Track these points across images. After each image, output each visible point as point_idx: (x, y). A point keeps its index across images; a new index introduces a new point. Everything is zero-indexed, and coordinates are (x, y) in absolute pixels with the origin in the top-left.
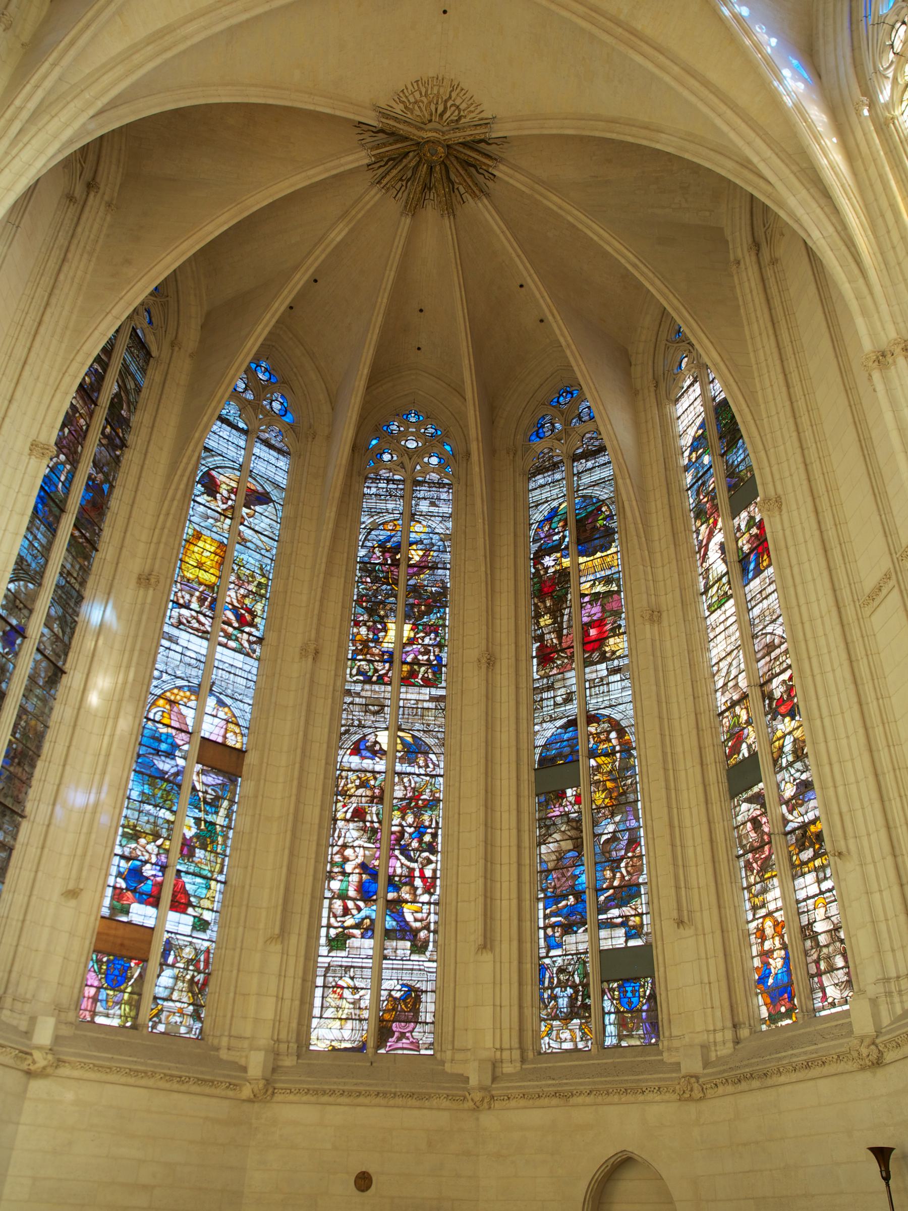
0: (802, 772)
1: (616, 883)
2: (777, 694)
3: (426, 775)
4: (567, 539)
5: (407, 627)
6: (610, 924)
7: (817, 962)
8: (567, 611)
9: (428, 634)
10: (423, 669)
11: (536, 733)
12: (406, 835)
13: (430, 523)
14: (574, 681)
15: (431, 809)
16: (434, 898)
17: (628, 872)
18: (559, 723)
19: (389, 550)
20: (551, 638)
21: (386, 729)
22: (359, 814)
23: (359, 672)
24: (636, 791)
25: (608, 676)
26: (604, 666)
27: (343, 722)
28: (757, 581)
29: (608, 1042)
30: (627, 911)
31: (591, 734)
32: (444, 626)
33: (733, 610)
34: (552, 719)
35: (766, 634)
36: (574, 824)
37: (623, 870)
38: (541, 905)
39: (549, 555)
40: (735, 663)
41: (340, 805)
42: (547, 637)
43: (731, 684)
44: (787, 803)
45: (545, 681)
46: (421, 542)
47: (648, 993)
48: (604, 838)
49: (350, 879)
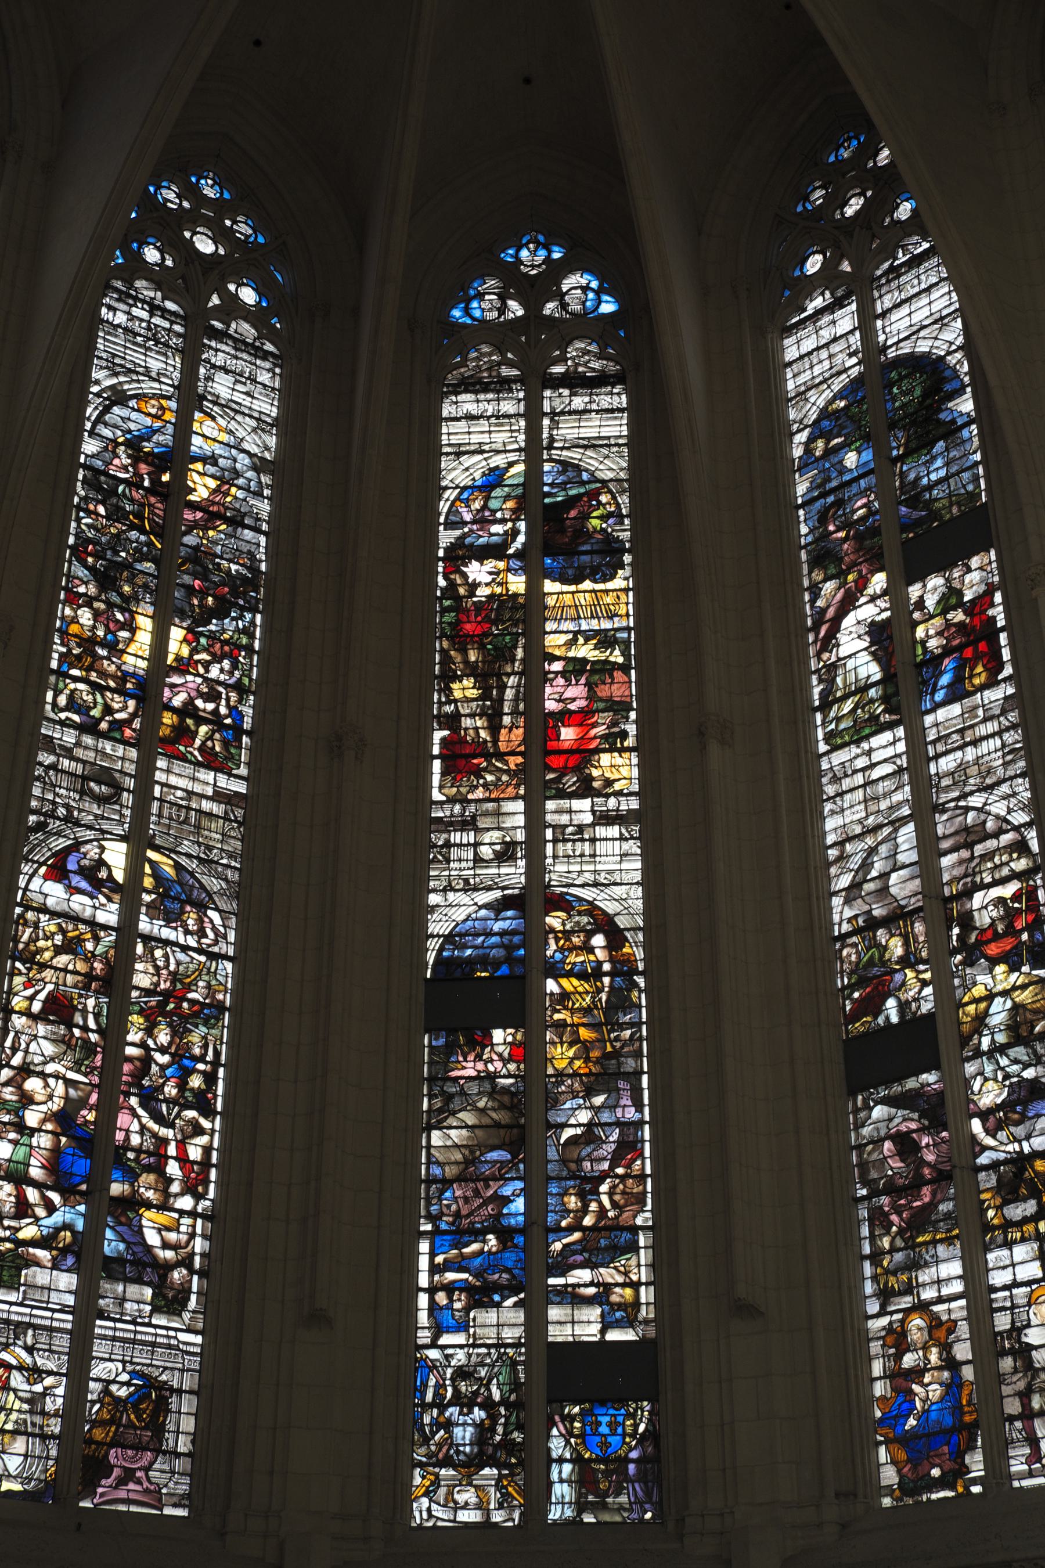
0: (1026, 1066)
1: (588, 1221)
2: (983, 919)
3: (200, 951)
4: (521, 539)
5: (177, 634)
6: (572, 1297)
7: (1025, 1396)
8: (512, 681)
9: (217, 659)
10: (203, 729)
11: (433, 908)
12: (154, 1069)
13: (233, 425)
14: (520, 820)
16: (204, 1205)
17: (614, 1204)
18: (484, 897)
19: (150, 458)
20: (474, 726)
21: (123, 838)
22: (59, 1009)
23: (73, 704)
24: (638, 1055)
25: (593, 825)
26: (585, 804)
27: (34, 803)
28: (956, 709)
29: (555, 1514)
30: (608, 1275)
31: (552, 930)
32: (250, 650)
33: (904, 749)
34: (469, 888)
35: (967, 809)
36: (506, 1099)
37: (605, 1200)
38: (424, 1246)
39: (481, 560)
40: (883, 850)
41: (18, 980)
42: (467, 722)
43: (869, 887)
44: (984, 1115)
45: (457, 808)
46: (211, 460)
47: (642, 1428)
48: (567, 1133)
49: (34, 1141)
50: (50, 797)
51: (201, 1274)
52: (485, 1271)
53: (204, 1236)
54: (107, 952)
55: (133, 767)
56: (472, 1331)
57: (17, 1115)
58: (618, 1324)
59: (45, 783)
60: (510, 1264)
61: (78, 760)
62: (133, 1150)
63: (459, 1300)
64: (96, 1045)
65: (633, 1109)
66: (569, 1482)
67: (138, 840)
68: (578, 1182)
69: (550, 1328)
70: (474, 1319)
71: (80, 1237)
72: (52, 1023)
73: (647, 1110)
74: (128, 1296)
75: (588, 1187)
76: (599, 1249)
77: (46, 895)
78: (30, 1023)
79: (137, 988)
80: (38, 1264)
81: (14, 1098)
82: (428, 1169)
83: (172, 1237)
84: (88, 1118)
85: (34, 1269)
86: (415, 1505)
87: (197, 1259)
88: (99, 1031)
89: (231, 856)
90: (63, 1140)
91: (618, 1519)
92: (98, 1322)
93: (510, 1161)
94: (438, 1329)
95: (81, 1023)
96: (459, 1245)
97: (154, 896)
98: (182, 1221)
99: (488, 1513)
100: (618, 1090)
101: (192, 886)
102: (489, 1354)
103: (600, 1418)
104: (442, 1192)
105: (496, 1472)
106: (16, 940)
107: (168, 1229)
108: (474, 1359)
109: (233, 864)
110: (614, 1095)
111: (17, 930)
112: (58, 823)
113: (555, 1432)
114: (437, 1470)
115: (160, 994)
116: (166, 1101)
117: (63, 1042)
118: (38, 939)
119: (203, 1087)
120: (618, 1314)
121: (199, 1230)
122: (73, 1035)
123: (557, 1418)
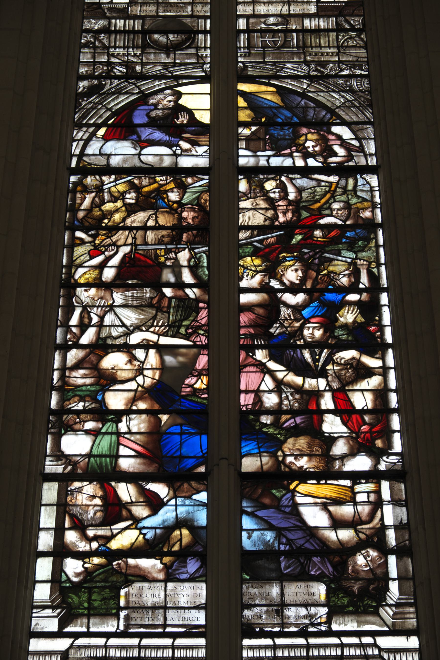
3: (326, 170)
12: (284, 312)
15: (351, 246)
21: (202, 80)
22: (139, 272)
27: (83, 70)
49: (123, 427)
50: (104, 59)
51: (400, 552)
53: (395, 502)
54: (198, 198)
55: (208, 8)
57: (94, 399)
59: (95, 47)
61: (134, 17)
62: (268, 412)
64: (197, 300)
67: (223, 80)
71: (203, 533)
72: (133, 287)
74: (288, 598)
77: (109, 156)
78: (102, 293)
79: (246, 228)
80: (144, 577)
81: (88, 381)
83: (347, 511)
84: (198, 386)
85: (138, 585)
87: (391, 535)
88: (200, 284)
89: (352, 65)
90: (164, 418)
92: (246, 642)
95: (172, 279)
97: (254, 128)
98: (358, 488)
101: (307, 107)
106: (74, 209)
107: (338, 502)
109: (358, 72)
111: (74, 199)
112: (116, 82)
115: (281, 227)
116: (310, 345)
117: (150, 305)
118: (103, 202)
119: (360, 319)
121: (386, 495)
122: (164, 295)
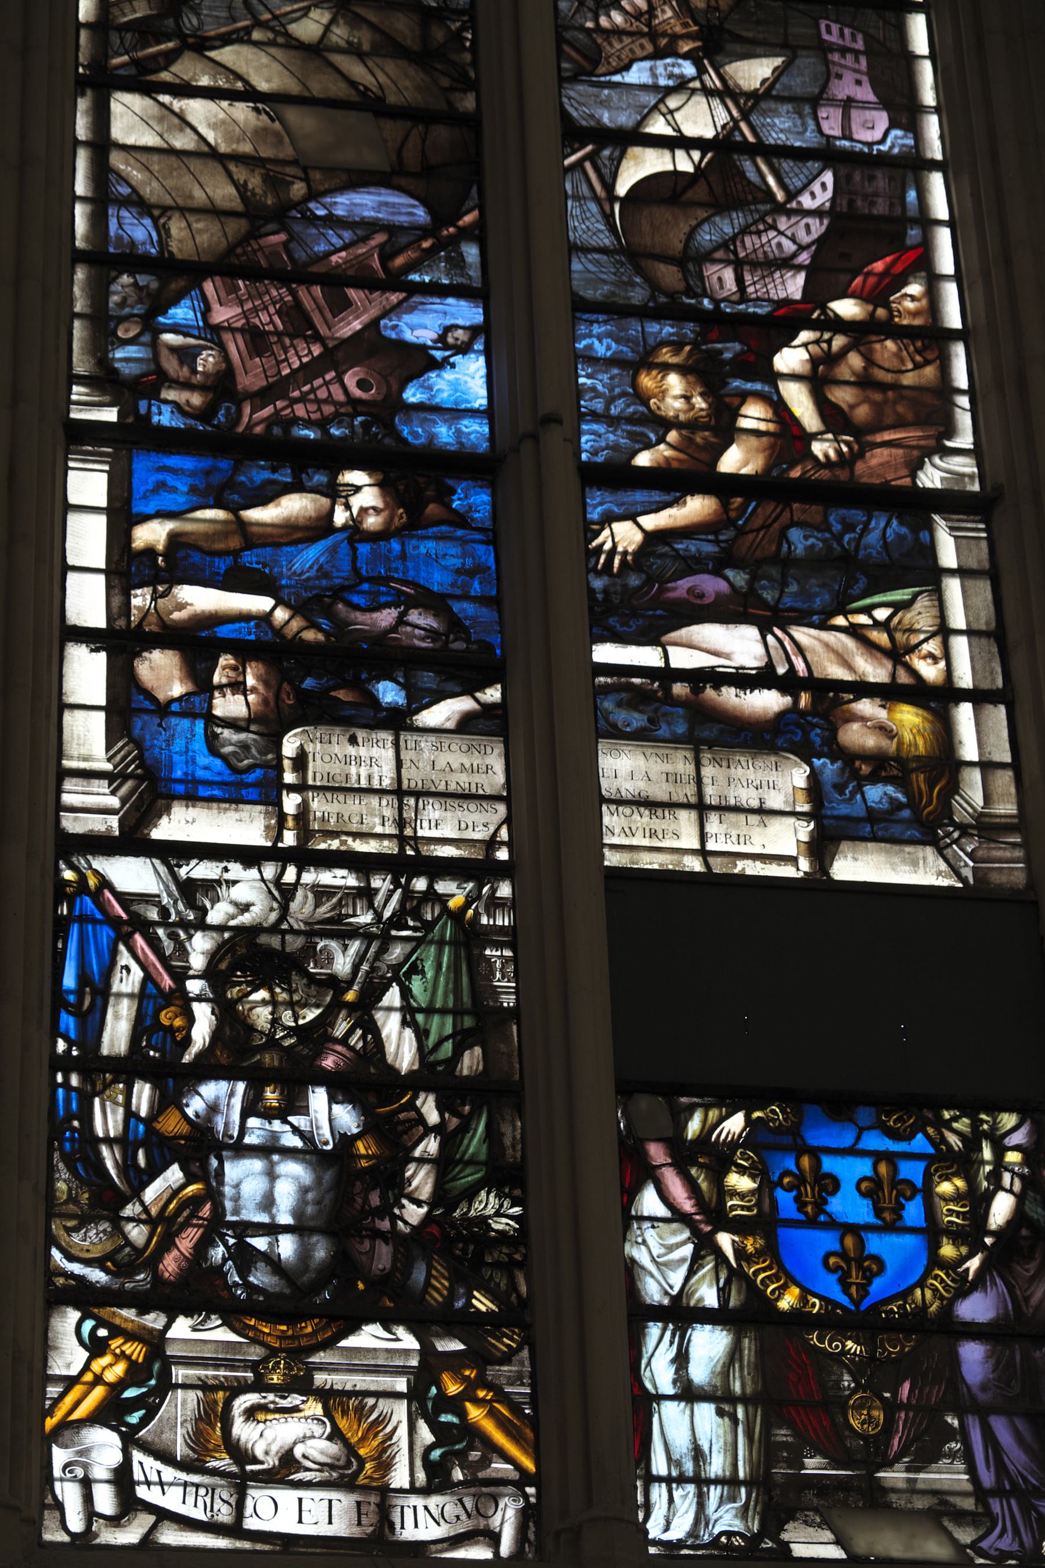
6: (691, 717)
17: (833, 418)
30: (826, 651)
37: (799, 400)
38: (88, 484)
47: (1001, 1208)
48: (640, 166)
52: (339, 593)
56: (291, 803)
58: (877, 829)
60: (438, 580)
63: (238, 687)
65: (882, 120)
66: (720, 1397)
68: (689, 329)
69: (610, 819)
70: (300, 762)
73: (932, 126)
75: (730, 350)
76: (787, 563)
82: (98, 220)
86: (60, 1456)
91: (935, 1549)
93: (425, 231)
94: (150, 788)
96: (236, 496)
99: (381, 1501)
100: (824, 49)
102: (367, 894)
103: (829, 1164)
104: (159, 304)
105: (409, 1341)
108: (302, 906)
110: (807, 62)
113: (650, 1202)
114: (154, 1320)
120: (875, 793)
123: (657, 1153)
